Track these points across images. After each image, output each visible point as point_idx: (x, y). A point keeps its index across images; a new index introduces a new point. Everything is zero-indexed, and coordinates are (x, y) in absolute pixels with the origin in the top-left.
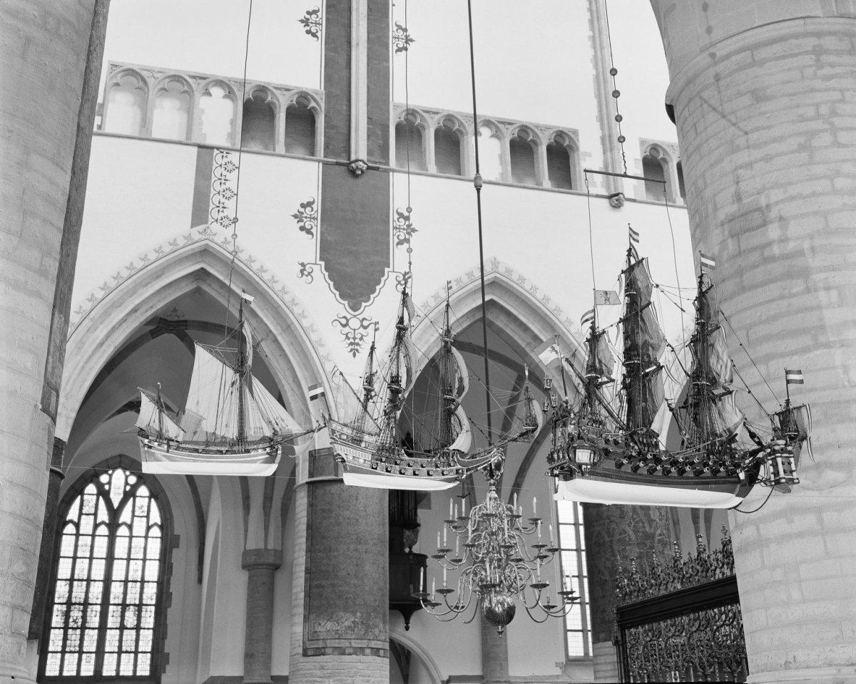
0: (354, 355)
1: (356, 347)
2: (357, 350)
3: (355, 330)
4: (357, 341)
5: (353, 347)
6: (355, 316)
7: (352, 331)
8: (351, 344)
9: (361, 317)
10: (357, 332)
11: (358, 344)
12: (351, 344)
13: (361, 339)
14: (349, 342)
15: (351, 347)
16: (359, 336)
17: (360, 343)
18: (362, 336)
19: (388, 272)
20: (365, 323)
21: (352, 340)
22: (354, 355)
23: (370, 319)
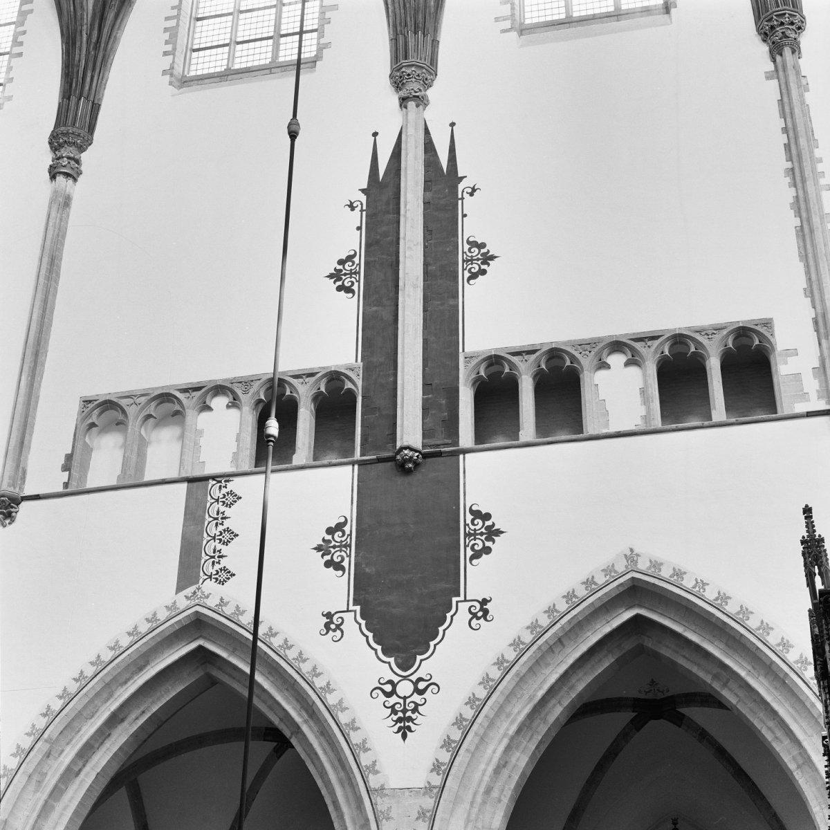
0: (404, 737)
1: (407, 724)
2: (409, 729)
3: (405, 698)
4: (409, 714)
5: (402, 724)
6: (405, 678)
7: (401, 701)
8: (399, 720)
9: (414, 678)
10: (408, 701)
11: (410, 719)
12: (399, 720)
13: (415, 710)
14: (395, 718)
15: (399, 725)
16: (412, 705)
17: (414, 716)
18: (417, 705)
19: (457, 602)
20: (422, 685)
21: (400, 714)
22: (404, 737)
23: (429, 677)
